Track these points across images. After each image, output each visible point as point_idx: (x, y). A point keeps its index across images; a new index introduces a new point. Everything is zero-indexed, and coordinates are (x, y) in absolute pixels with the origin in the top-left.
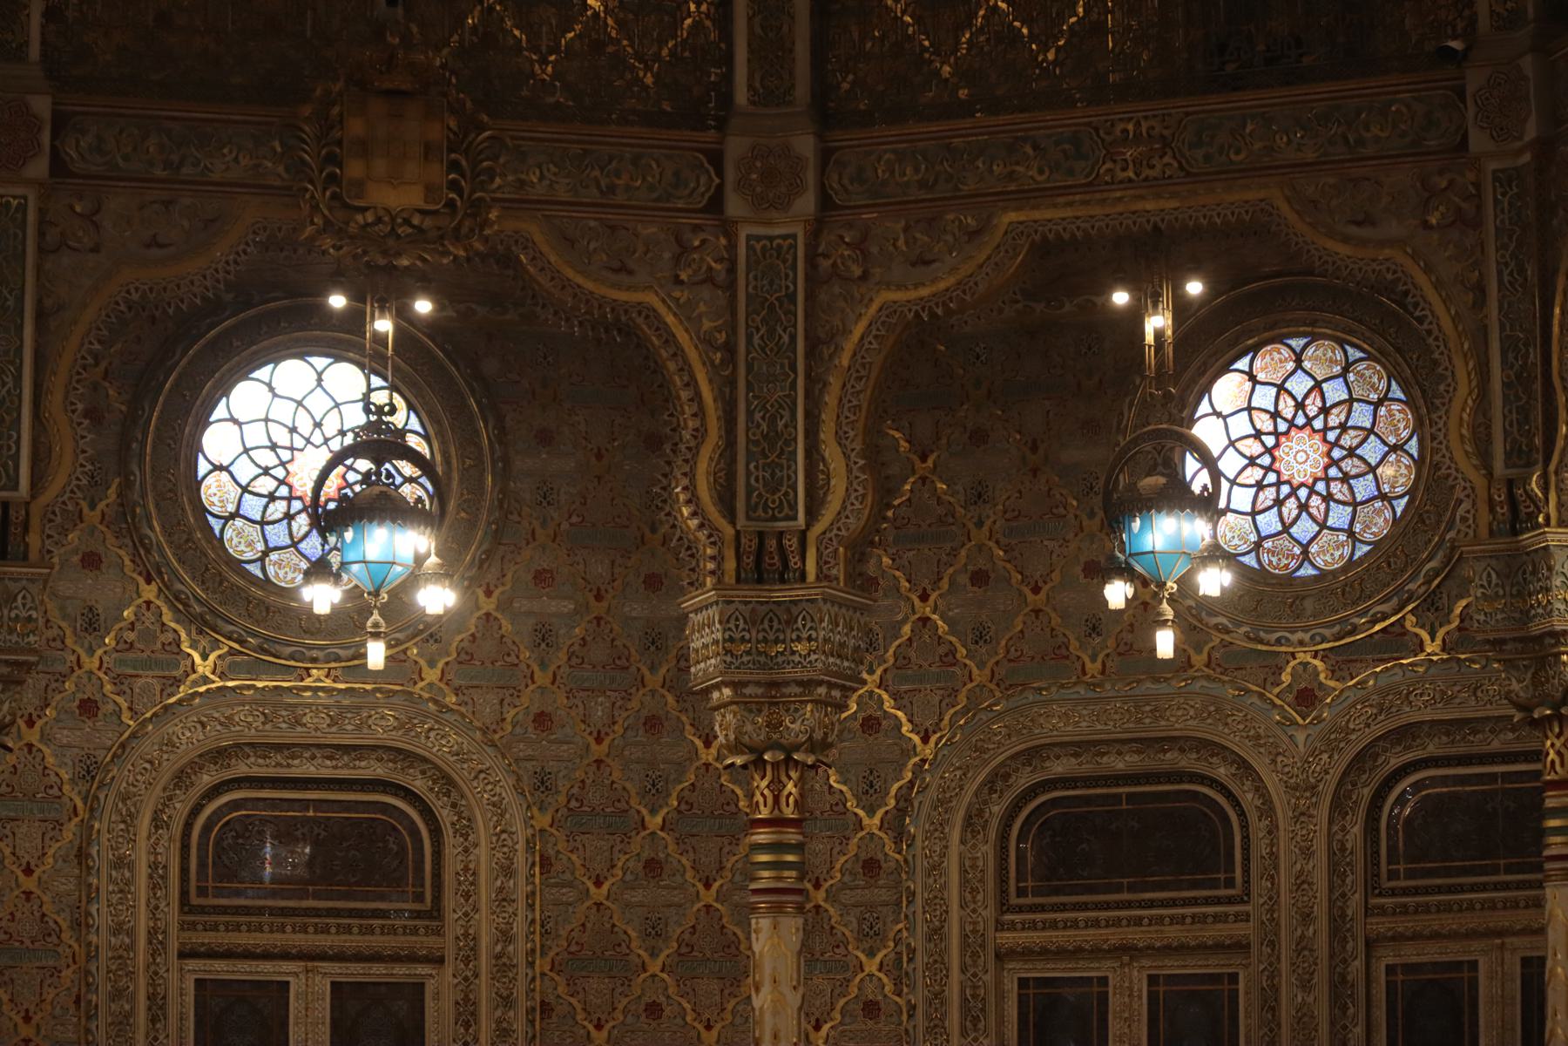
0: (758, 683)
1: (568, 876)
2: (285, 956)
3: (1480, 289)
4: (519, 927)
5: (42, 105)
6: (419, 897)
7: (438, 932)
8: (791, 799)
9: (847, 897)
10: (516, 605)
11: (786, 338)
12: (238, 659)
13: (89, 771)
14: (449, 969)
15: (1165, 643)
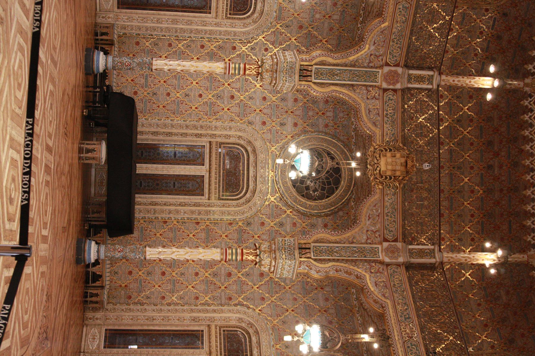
0: (275, 247)
1: (228, 229)
2: (210, 165)
4: (216, 217)
5: (398, 86)
8: (248, 257)
9: (223, 294)
10: (288, 218)
11: (356, 255)
12: (275, 157)
14: (207, 201)
15: (288, 338)
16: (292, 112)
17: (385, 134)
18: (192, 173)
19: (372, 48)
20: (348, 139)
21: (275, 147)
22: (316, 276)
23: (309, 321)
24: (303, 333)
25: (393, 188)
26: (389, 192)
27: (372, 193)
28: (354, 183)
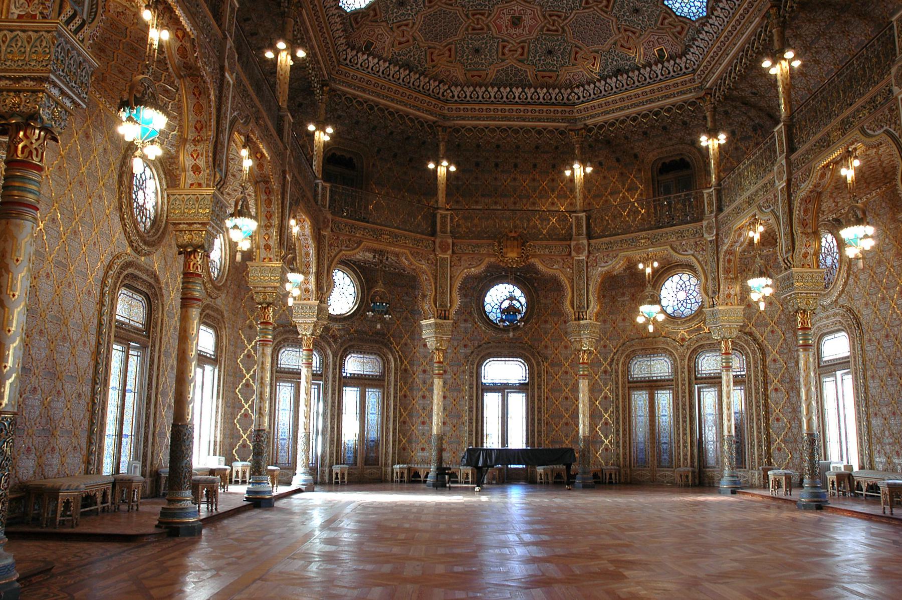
5: (450, 241)
19: (423, 262)
23: (636, 312)
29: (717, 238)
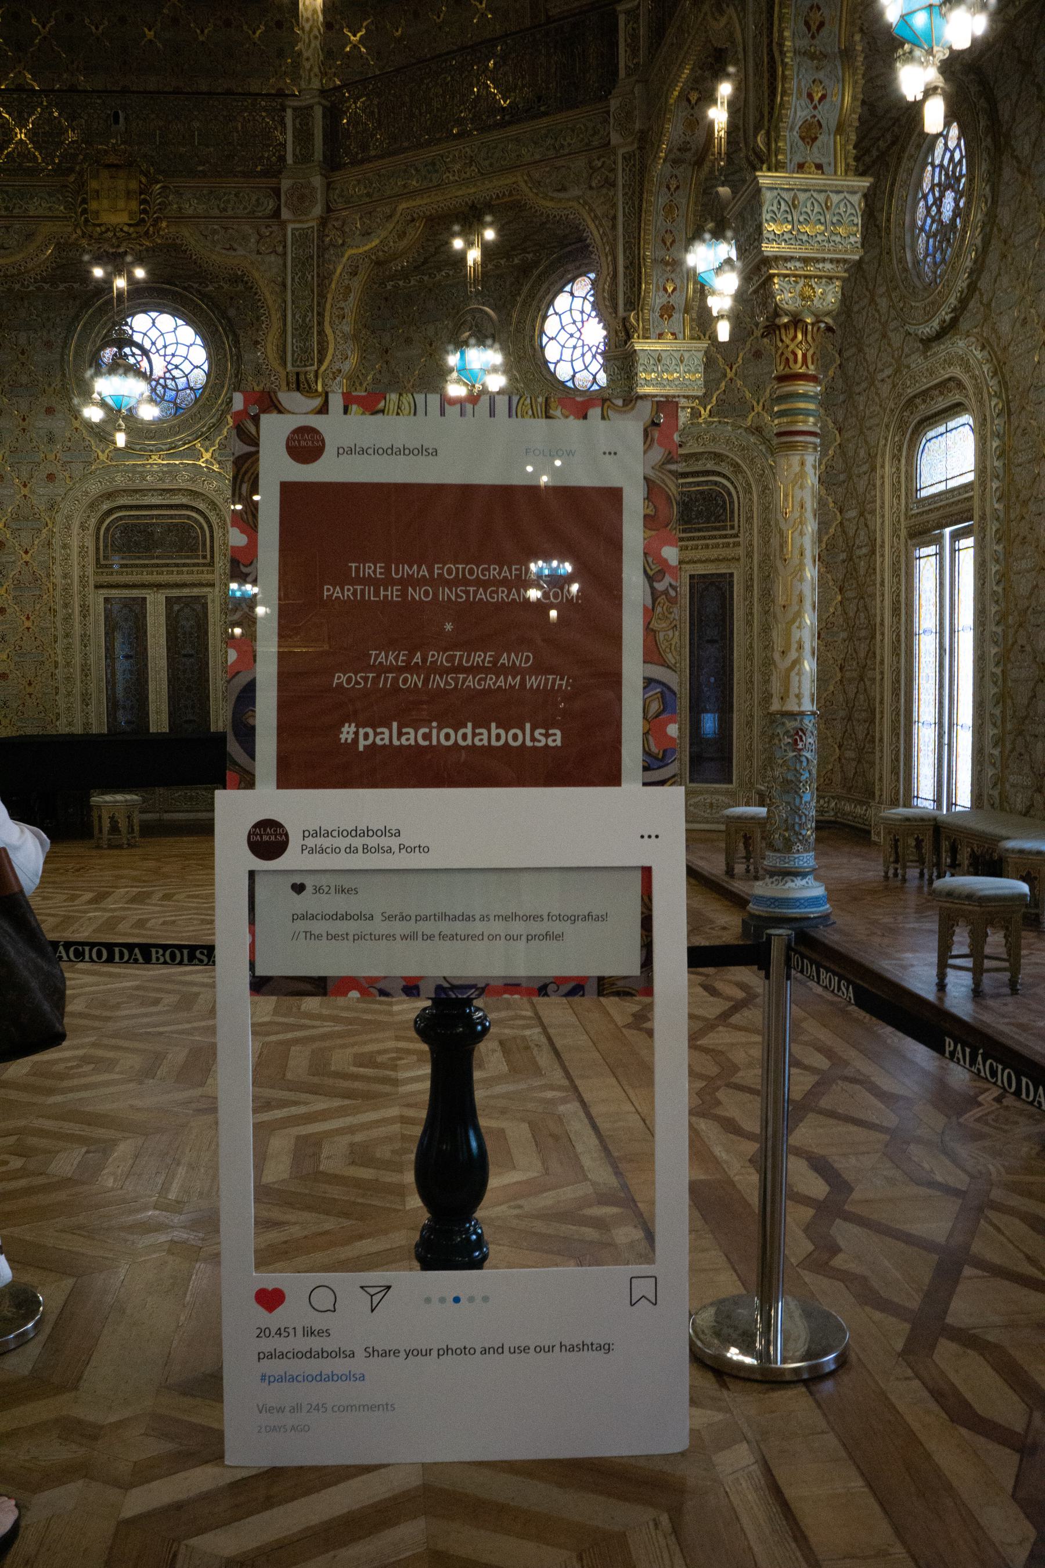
2: (143, 586)
3: (614, 218)
6: (204, 557)
7: (213, 572)
11: (310, 277)
13: (52, 507)
14: (217, 589)
16: (24, 420)
17: (50, 214)
18: (163, 620)
20: (75, 298)
21: (100, 454)
22: (353, 360)
24: (466, 384)
25: (167, 197)
26: (175, 206)
27: (178, 241)
28: (168, 284)
29: (641, 148)
